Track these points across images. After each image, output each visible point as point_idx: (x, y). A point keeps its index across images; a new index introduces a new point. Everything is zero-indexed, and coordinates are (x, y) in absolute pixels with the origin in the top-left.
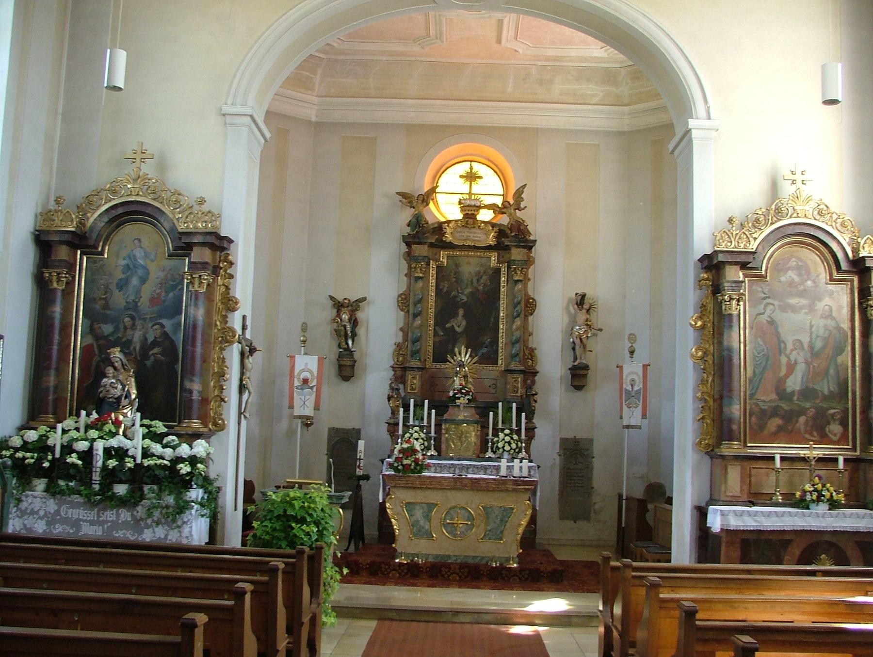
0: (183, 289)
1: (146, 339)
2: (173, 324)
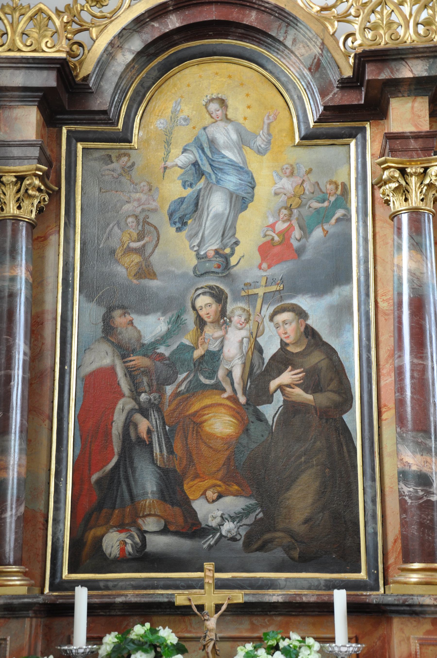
0: (347, 219)
1: (260, 351)
2: (331, 307)
